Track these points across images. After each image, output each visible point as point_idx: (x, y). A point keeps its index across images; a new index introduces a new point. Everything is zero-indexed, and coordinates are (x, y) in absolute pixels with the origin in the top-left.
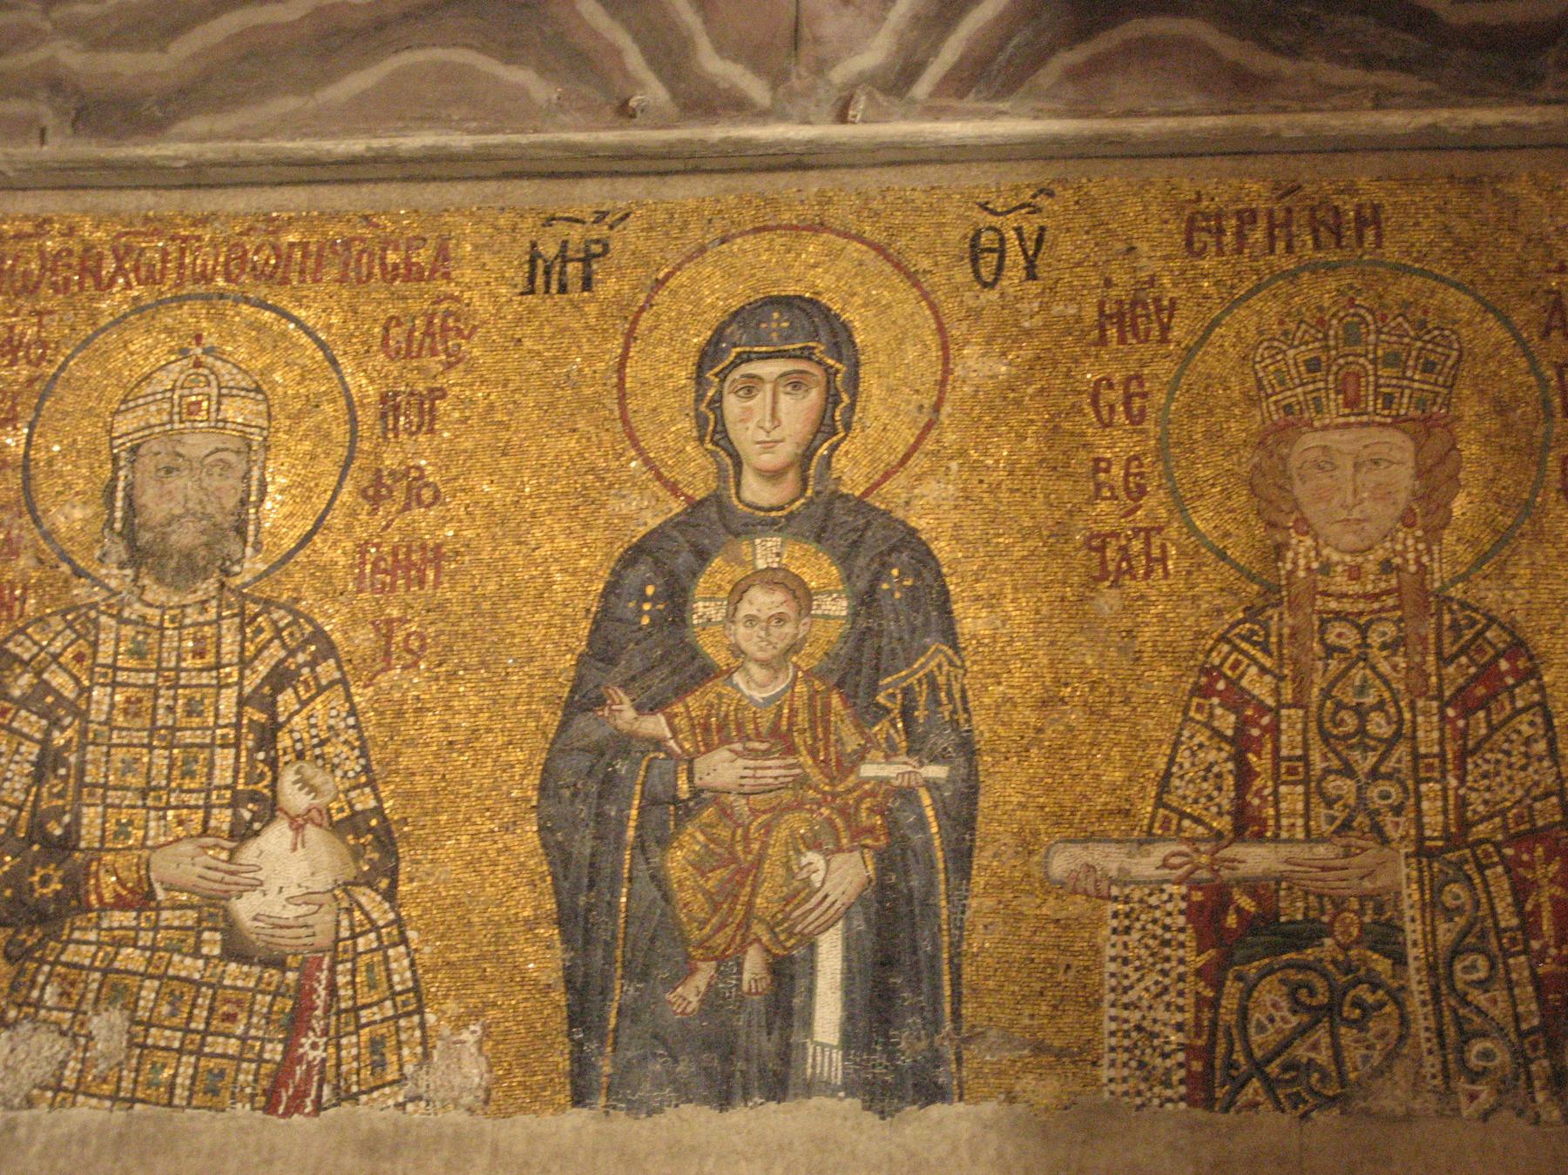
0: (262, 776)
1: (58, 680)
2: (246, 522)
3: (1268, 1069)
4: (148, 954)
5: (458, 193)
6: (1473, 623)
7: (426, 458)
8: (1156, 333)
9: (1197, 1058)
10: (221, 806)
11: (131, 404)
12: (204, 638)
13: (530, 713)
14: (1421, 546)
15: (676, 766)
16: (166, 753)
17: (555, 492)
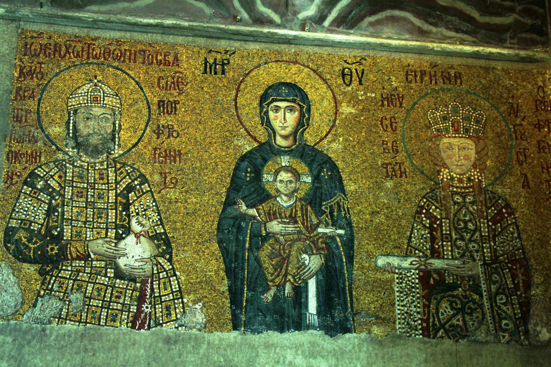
0: (125, 220)
1: (53, 183)
2: (115, 138)
3: (446, 326)
4: (89, 275)
5: (180, 39)
6: (495, 198)
7: (174, 122)
8: (398, 104)
9: (424, 322)
10: (112, 229)
11: (74, 96)
12: (103, 174)
13: (213, 205)
14: (479, 174)
15: (261, 225)
16: (92, 210)
17: (217, 137)
